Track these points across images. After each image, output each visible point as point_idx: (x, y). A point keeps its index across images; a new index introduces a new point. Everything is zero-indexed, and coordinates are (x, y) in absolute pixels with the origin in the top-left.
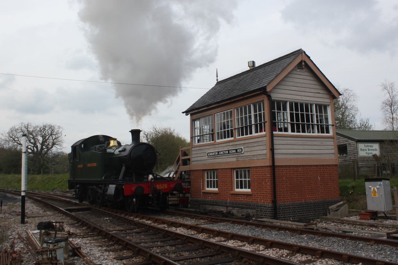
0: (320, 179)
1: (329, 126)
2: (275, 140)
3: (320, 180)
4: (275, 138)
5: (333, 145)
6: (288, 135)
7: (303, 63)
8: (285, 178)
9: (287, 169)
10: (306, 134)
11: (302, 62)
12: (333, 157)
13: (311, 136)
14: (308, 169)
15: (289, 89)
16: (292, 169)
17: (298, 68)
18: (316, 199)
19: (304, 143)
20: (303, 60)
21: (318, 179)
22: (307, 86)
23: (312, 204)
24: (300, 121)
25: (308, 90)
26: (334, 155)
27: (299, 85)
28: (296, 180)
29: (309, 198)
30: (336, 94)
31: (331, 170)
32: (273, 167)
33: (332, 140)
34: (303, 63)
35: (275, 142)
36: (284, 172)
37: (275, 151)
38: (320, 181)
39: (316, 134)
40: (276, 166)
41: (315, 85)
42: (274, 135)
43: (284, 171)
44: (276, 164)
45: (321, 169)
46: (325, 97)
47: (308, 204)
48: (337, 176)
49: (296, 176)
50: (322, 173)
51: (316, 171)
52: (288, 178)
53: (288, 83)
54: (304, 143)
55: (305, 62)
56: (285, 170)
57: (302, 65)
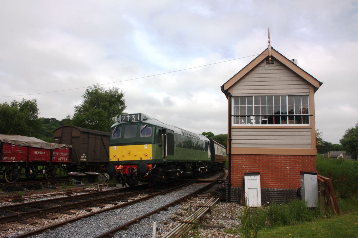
0: (289, 168)
1: (309, 116)
2: (233, 132)
3: (288, 169)
4: (233, 130)
5: (310, 135)
6: (253, 126)
7: (270, 59)
8: (244, 165)
9: (248, 158)
10: (281, 125)
11: (269, 58)
12: (309, 147)
13: (274, 127)
14: (274, 158)
15: (266, 82)
16: (253, 158)
17: (267, 64)
18: (281, 188)
19: (269, 133)
20: (270, 55)
21: (286, 168)
22: (277, 79)
23: (275, 191)
24: (247, 114)
25: (280, 83)
26: (310, 145)
27: (266, 79)
28: (257, 168)
29: (272, 185)
30: (316, 85)
31: (306, 161)
32: (230, 155)
33: (309, 130)
34: (270, 59)
35: (233, 133)
36: (244, 160)
37: (233, 142)
38: (289, 170)
39: (288, 125)
40: (232, 154)
41: (289, 77)
42: (232, 128)
43: (243, 159)
44: (233, 152)
45: (292, 159)
46: (306, 88)
47: (270, 191)
48: (314, 167)
49: (261, 164)
50: (292, 163)
51: (284, 161)
52: (247, 165)
53: (253, 80)
54: (269, 133)
55: (272, 57)
56: (244, 158)
57: (269, 61)
